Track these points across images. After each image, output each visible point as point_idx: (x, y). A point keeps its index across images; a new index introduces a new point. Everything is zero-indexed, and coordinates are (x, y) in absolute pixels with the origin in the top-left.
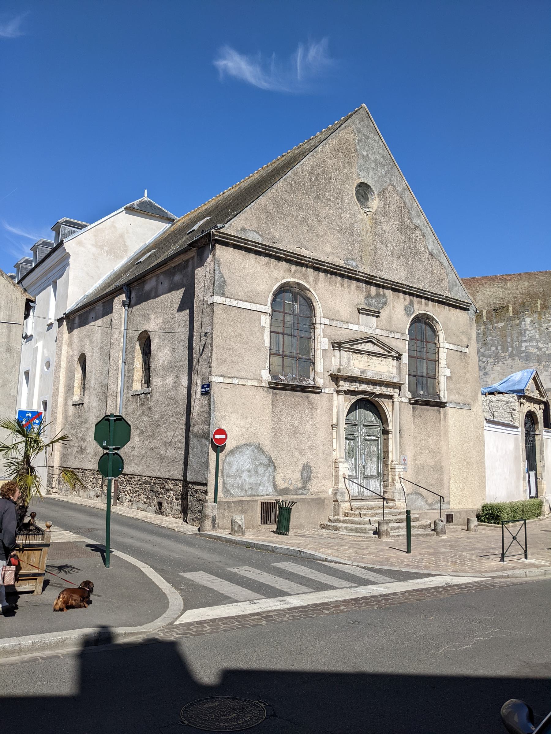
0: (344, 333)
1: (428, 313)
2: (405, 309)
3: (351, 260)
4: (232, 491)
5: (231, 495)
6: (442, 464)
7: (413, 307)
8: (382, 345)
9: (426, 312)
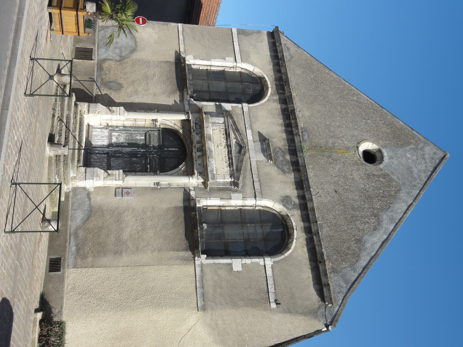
0: (241, 125)
1: (295, 231)
2: (287, 197)
3: (308, 135)
4: (102, 32)
5: (99, 31)
6: (124, 254)
7: (294, 208)
8: (241, 161)
9: (295, 228)
